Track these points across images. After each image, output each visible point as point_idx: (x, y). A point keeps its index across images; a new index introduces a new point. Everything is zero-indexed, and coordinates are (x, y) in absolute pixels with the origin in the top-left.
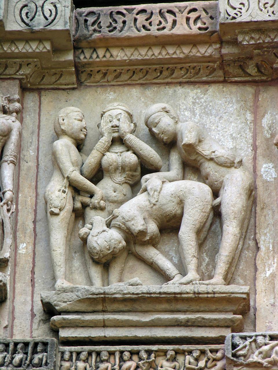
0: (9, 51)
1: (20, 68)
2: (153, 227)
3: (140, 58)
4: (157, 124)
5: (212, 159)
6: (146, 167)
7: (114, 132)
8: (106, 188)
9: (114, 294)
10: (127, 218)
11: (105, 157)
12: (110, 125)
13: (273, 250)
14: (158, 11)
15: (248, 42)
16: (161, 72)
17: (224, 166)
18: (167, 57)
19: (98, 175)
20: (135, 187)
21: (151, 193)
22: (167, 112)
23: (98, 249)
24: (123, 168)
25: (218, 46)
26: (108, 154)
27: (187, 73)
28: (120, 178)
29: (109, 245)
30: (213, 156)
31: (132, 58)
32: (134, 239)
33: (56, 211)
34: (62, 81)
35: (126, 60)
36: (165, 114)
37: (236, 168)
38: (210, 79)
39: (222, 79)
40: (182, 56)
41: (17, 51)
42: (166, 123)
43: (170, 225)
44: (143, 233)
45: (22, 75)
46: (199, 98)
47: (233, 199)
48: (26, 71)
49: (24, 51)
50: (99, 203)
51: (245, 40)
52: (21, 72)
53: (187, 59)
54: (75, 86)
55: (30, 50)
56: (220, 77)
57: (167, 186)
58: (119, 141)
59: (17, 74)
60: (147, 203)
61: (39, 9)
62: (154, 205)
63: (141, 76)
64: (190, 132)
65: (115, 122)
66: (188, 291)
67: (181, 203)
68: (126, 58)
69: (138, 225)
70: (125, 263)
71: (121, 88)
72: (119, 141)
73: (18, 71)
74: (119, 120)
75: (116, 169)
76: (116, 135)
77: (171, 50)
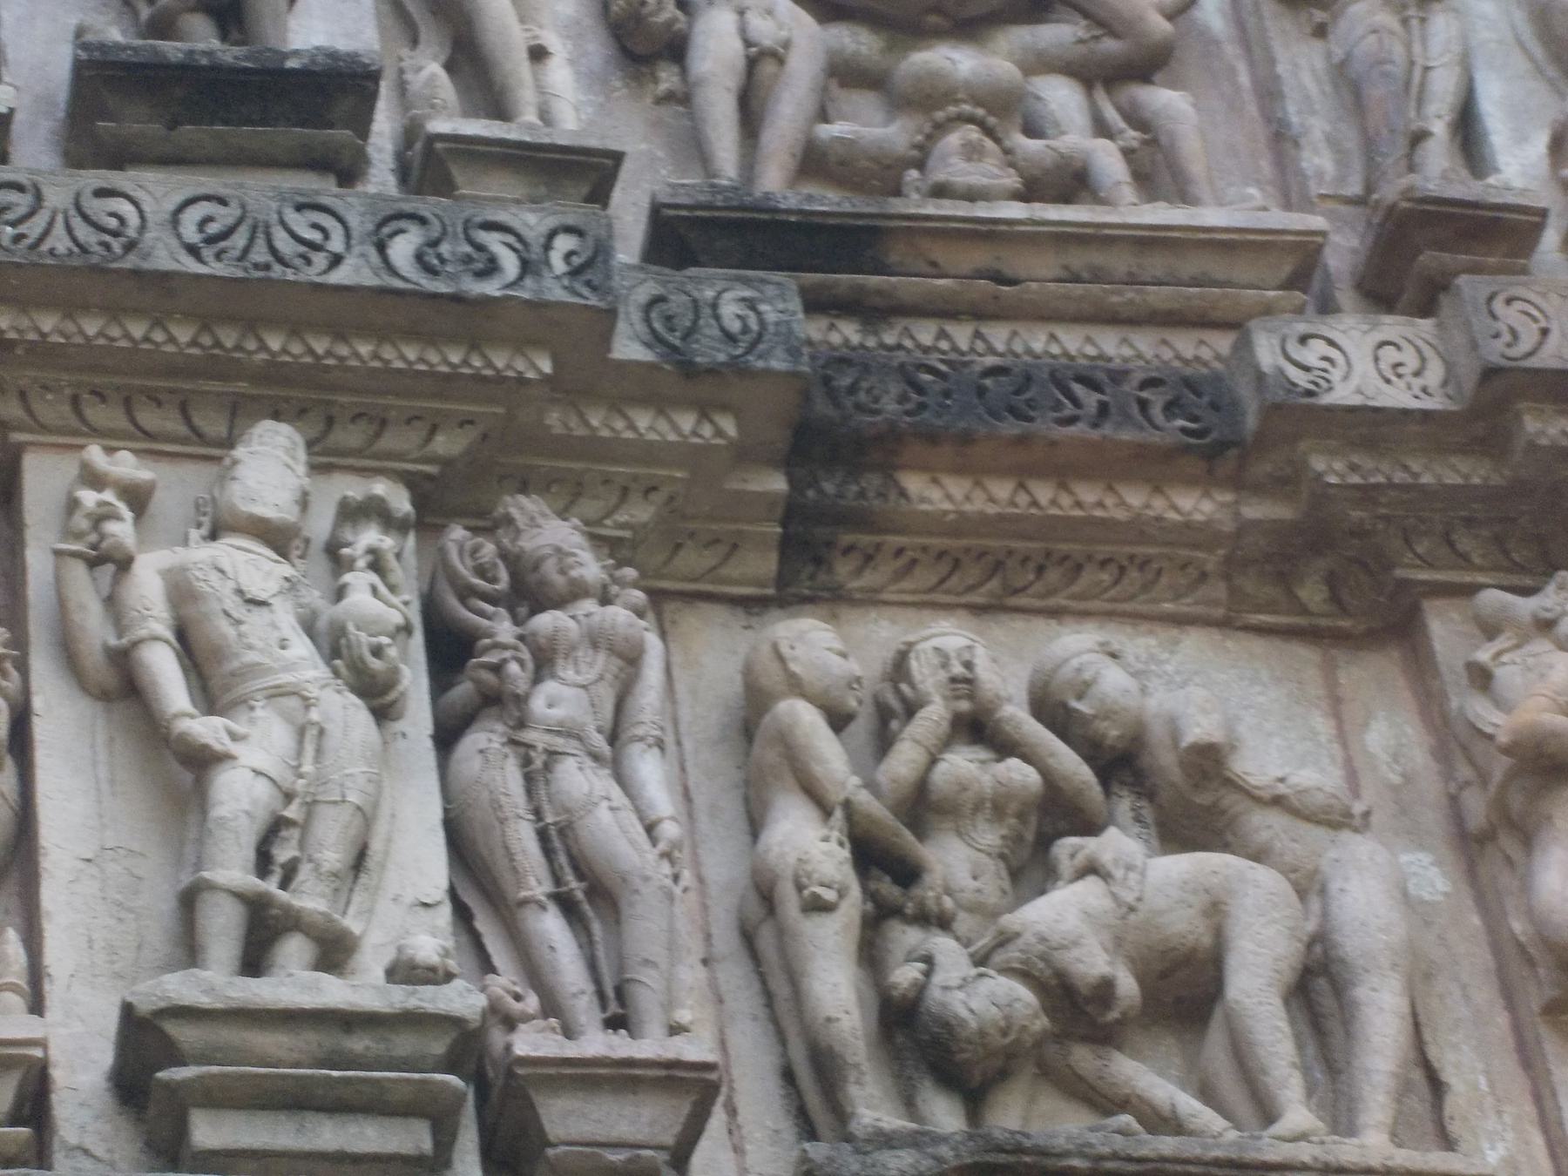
0: (605, 433)
1: (616, 508)
2: (1128, 985)
3: (991, 509)
4: (1087, 685)
5: (1278, 802)
7: (958, 698)
9: (1066, 1154)
10: (1055, 939)
11: (942, 767)
12: (943, 675)
13: (1493, 1093)
14: (1046, 376)
15: (1342, 476)
16: (1040, 570)
17: (1319, 823)
18: (1077, 513)
21: (1119, 873)
22: (1114, 656)
23: (973, 1024)
24: (998, 805)
25: (1228, 497)
26: (947, 756)
27: (1116, 582)
28: (990, 836)
29: (1007, 1018)
30: (1282, 789)
31: (967, 507)
32: (1075, 1008)
33: (829, 895)
34: (730, 570)
35: (946, 513)
36: (1108, 660)
37: (1356, 830)
38: (1185, 609)
39: (1219, 612)
40: (1121, 515)
41: (629, 435)
44: (1105, 990)
45: (622, 526)
46: (1160, 663)
48: (640, 512)
49: (653, 436)
50: (938, 898)
51: (1330, 467)
52: (622, 517)
53: (1139, 529)
54: (770, 591)
55: (672, 437)
56: (1215, 603)
58: (977, 727)
59: (608, 522)
60: (1108, 903)
61: (707, 311)
62: (1132, 909)
63: (971, 582)
64: (1204, 711)
65: (958, 669)
66: (1307, 1159)
67: (1216, 910)
68: (947, 506)
69: (1093, 961)
70: (1032, 1100)
71: (911, 613)
72: (977, 727)
73: (608, 515)
74: (968, 665)
75: (977, 807)
76: (964, 706)
77: (1088, 493)
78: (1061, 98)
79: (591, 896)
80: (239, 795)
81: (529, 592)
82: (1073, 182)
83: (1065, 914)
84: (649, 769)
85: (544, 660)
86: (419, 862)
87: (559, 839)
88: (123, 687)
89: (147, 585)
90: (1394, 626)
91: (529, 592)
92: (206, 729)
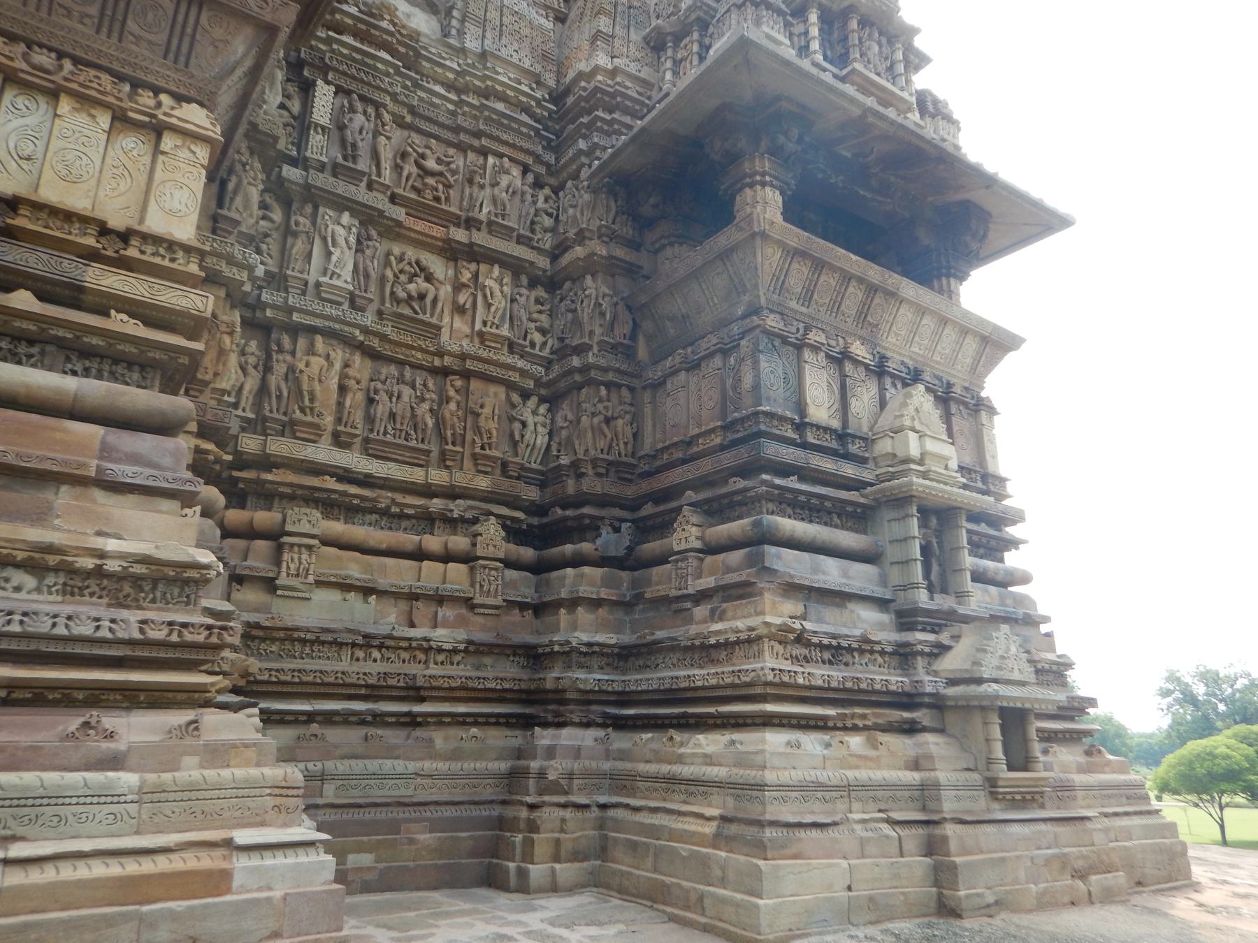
6: (415, 275)
8: (403, 278)
19: (401, 271)
20: (410, 281)
32: (410, 297)
42: (424, 262)
43: (422, 297)
47: (442, 293)
57: (421, 284)
58: (410, 264)
69: (414, 294)
78: (440, 187)
79: (367, 276)
80: (334, 258)
81: (369, 238)
82: (437, 199)
83: (412, 287)
84: (376, 262)
85: (368, 247)
86: (350, 267)
87: (365, 270)
88: (324, 239)
89: (330, 230)
90: (455, 260)
91: (369, 238)
92: (332, 249)
